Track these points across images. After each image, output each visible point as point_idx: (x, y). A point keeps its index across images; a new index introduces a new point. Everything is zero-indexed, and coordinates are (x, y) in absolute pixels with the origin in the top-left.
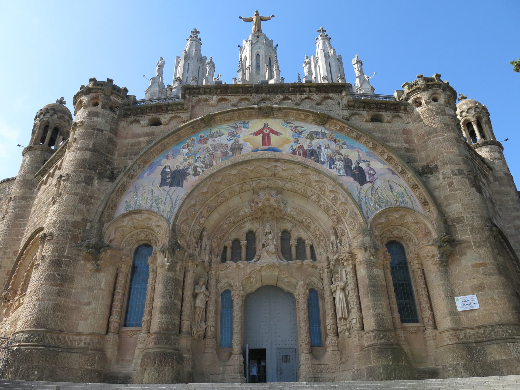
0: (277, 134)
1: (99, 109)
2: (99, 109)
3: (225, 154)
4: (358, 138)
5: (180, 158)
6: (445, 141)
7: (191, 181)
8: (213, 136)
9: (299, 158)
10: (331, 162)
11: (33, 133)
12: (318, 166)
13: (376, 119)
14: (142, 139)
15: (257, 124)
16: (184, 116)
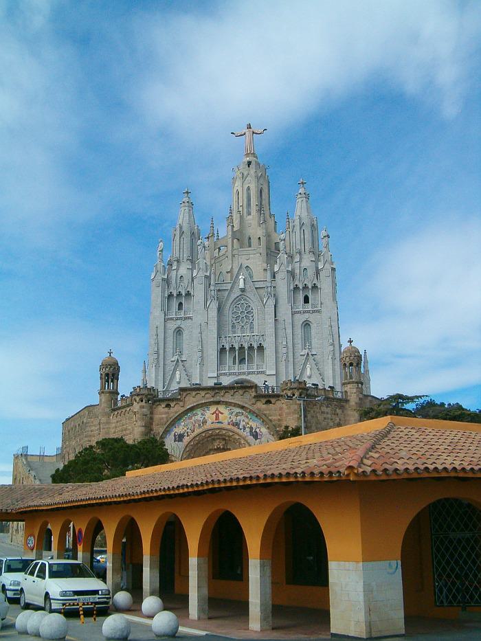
0: (222, 413)
1: (143, 403)
2: (143, 403)
3: (199, 425)
4: (256, 416)
5: (181, 427)
6: (293, 419)
7: (186, 439)
8: (194, 415)
9: (230, 427)
10: (244, 428)
11: (101, 378)
12: (238, 431)
13: (269, 402)
14: (164, 416)
15: (213, 409)
16: (181, 403)
